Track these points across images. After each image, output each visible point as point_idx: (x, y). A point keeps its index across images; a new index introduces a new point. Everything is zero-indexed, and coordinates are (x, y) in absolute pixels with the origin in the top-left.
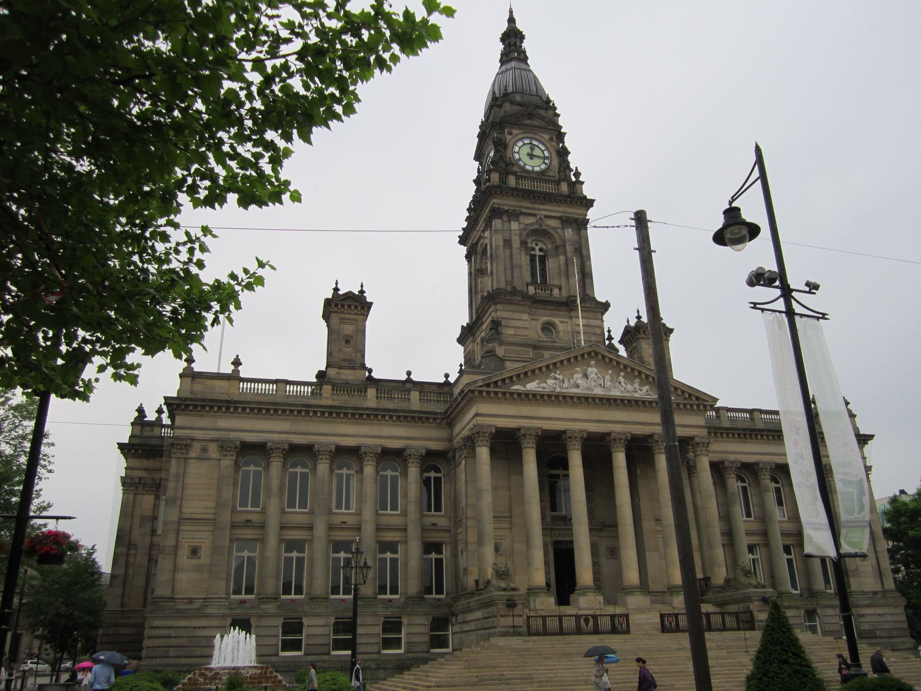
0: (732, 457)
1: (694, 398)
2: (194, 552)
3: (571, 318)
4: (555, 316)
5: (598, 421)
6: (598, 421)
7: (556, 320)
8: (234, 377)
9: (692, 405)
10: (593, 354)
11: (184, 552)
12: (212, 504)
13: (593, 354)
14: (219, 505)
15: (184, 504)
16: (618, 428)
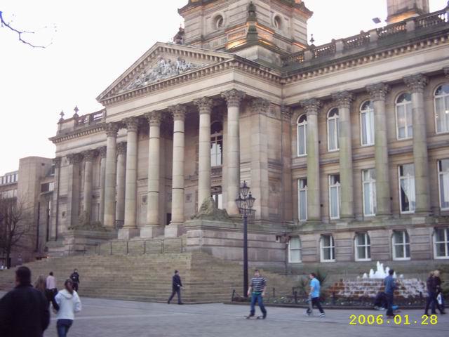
0: (342, 88)
1: (220, 60)
2: (63, 214)
3: (228, 5)
4: (220, 8)
5: (164, 101)
6: (164, 101)
7: (220, 12)
8: (76, 117)
9: (218, 66)
10: (160, 49)
11: (60, 215)
12: (67, 190)
13: (160, 49)
14: (69, 190)
15: (60, 191)
16: (175, 102)
